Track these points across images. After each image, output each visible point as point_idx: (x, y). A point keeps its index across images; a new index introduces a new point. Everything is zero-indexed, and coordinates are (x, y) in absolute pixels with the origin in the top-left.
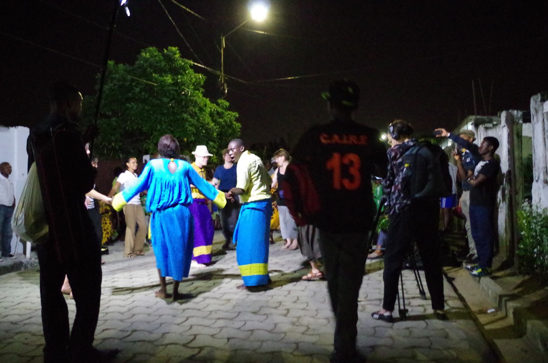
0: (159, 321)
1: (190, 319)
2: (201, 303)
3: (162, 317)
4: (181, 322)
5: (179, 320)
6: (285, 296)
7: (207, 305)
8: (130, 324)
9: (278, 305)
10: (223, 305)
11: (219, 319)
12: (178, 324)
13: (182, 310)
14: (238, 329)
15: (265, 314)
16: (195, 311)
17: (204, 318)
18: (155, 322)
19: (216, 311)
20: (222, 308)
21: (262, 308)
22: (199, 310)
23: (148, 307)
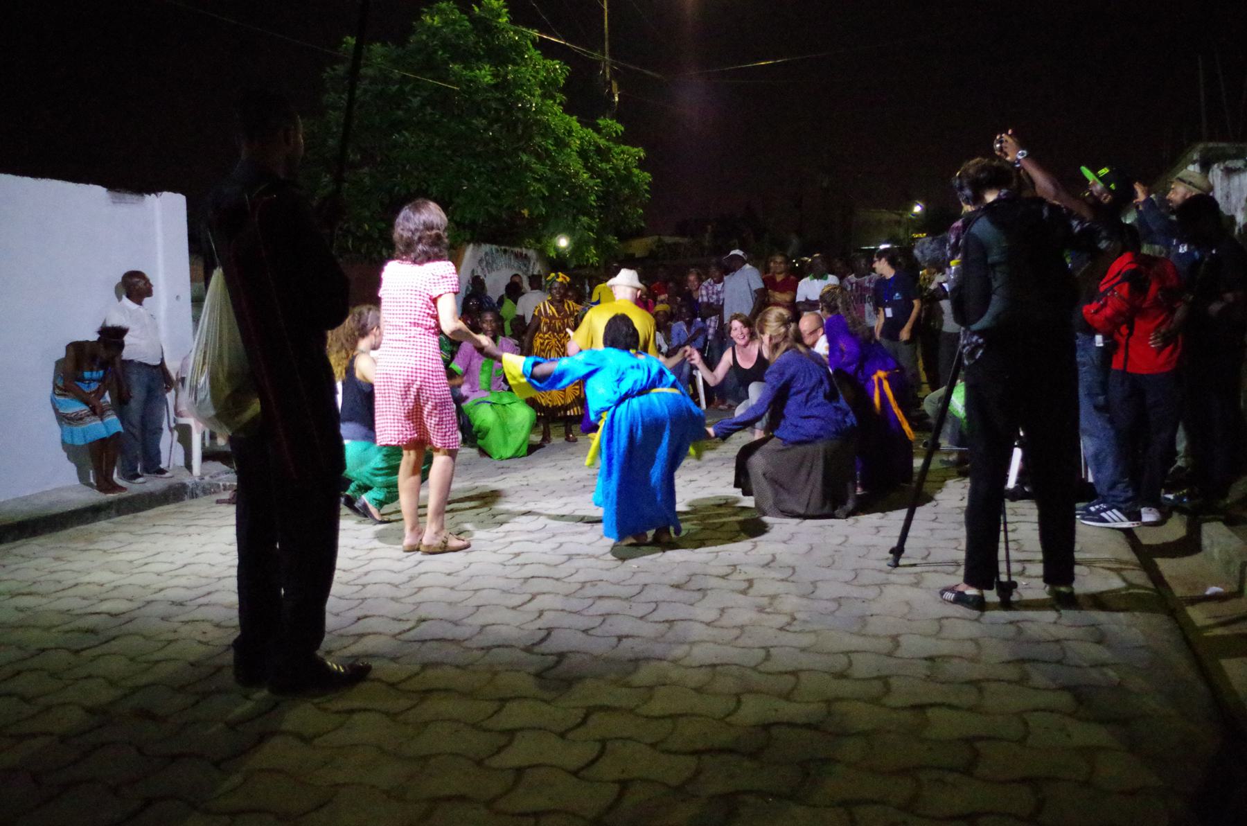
0: (474, 602)
1: (540, 598)
2: (561, 566)
3: (479, 594)
4: (520, 603)
5: (516, 600)
6: (746, 553)
7: (575, 571)
8: (412, 607)
9: (729, 570)
10: (608, 570)
11: (600, 597)
12: (514, 608)
13: (522, 580)
14: (641, 618)
15: (699, 590)
16: (549, 581)
17: (567, 596)
18: (464, 603)
19: (594, 583)
20: (606, 576)
21: (693, 578)
22: (558, 579)
23: (449, 574)
